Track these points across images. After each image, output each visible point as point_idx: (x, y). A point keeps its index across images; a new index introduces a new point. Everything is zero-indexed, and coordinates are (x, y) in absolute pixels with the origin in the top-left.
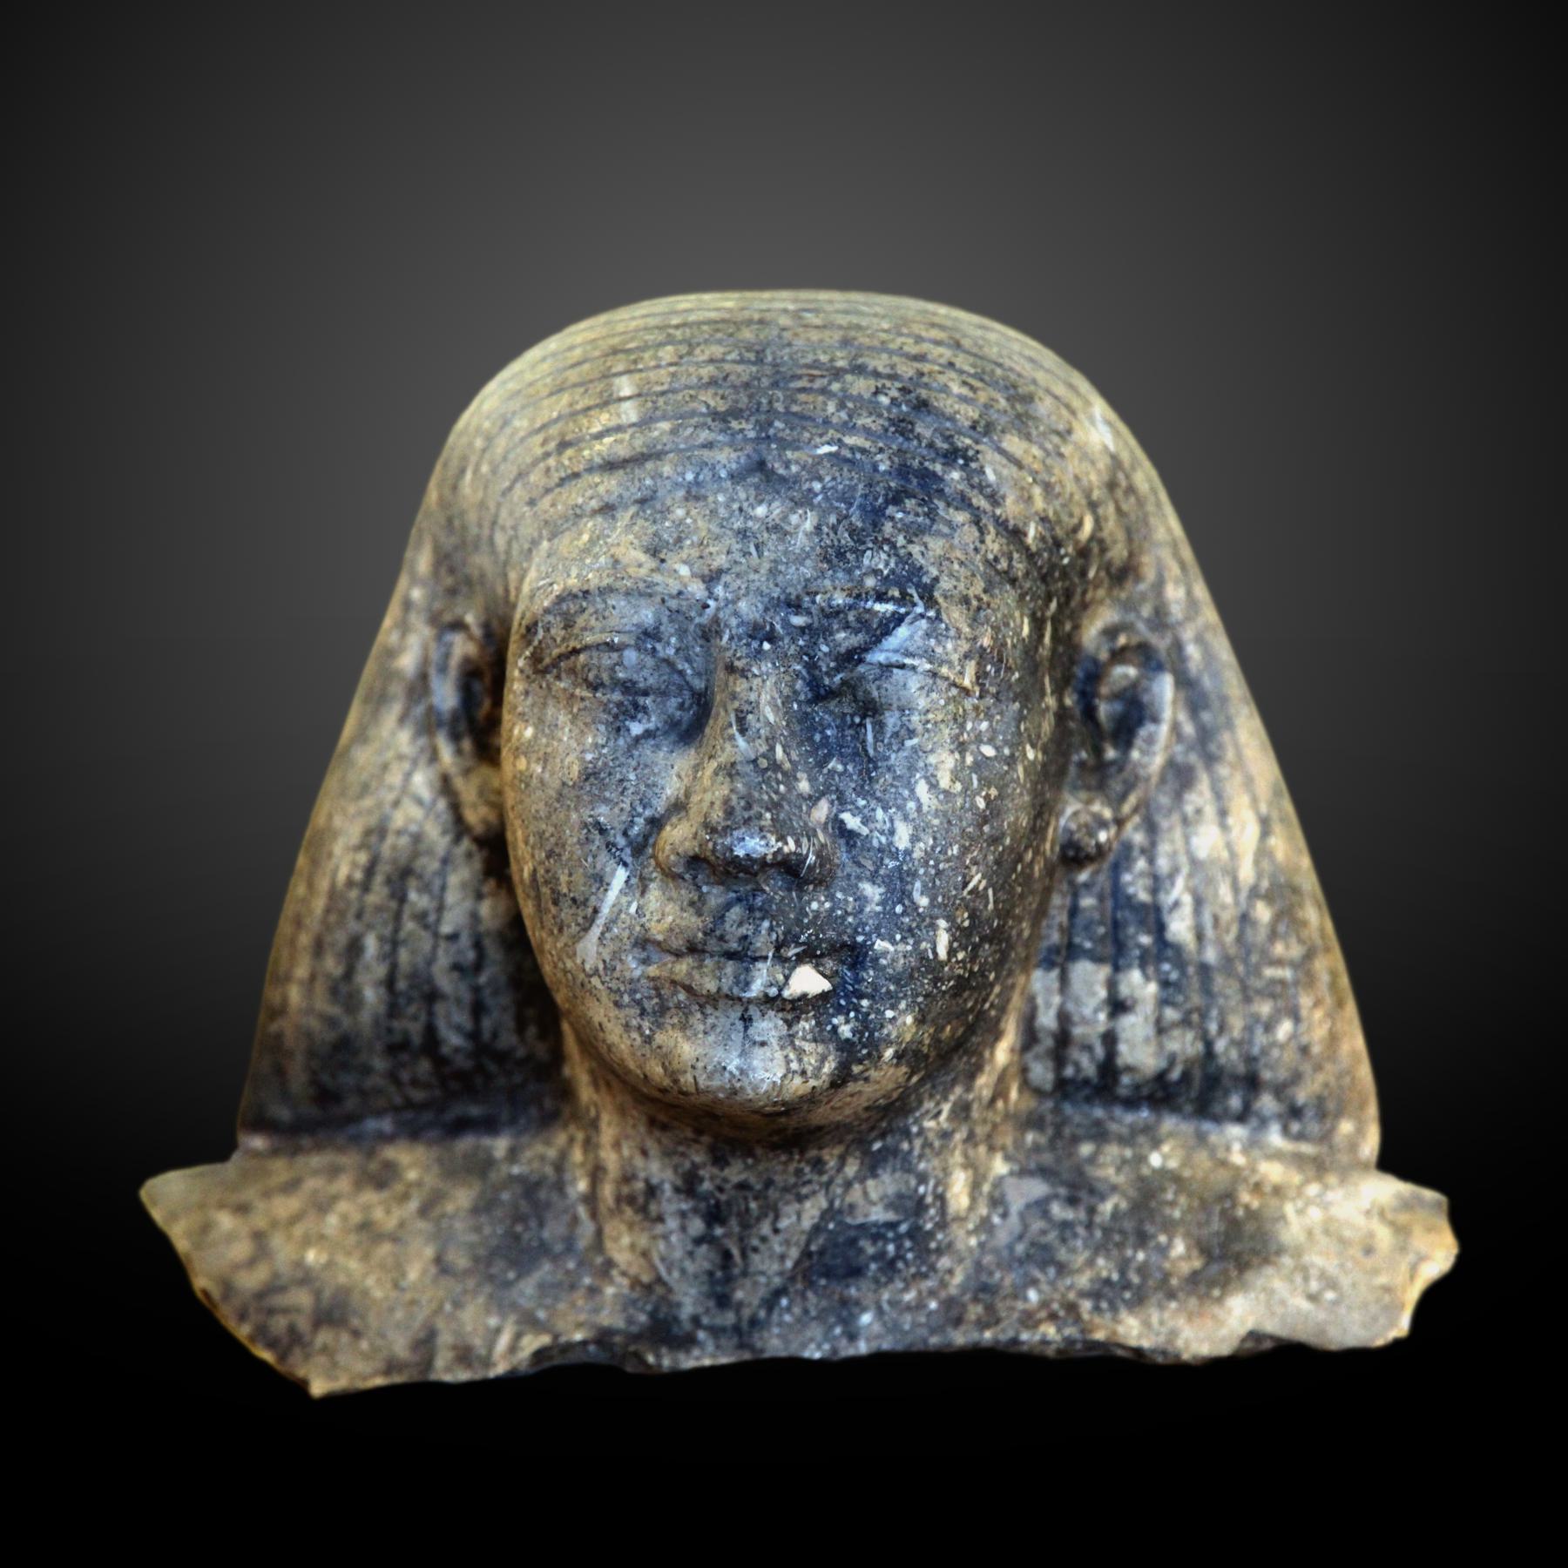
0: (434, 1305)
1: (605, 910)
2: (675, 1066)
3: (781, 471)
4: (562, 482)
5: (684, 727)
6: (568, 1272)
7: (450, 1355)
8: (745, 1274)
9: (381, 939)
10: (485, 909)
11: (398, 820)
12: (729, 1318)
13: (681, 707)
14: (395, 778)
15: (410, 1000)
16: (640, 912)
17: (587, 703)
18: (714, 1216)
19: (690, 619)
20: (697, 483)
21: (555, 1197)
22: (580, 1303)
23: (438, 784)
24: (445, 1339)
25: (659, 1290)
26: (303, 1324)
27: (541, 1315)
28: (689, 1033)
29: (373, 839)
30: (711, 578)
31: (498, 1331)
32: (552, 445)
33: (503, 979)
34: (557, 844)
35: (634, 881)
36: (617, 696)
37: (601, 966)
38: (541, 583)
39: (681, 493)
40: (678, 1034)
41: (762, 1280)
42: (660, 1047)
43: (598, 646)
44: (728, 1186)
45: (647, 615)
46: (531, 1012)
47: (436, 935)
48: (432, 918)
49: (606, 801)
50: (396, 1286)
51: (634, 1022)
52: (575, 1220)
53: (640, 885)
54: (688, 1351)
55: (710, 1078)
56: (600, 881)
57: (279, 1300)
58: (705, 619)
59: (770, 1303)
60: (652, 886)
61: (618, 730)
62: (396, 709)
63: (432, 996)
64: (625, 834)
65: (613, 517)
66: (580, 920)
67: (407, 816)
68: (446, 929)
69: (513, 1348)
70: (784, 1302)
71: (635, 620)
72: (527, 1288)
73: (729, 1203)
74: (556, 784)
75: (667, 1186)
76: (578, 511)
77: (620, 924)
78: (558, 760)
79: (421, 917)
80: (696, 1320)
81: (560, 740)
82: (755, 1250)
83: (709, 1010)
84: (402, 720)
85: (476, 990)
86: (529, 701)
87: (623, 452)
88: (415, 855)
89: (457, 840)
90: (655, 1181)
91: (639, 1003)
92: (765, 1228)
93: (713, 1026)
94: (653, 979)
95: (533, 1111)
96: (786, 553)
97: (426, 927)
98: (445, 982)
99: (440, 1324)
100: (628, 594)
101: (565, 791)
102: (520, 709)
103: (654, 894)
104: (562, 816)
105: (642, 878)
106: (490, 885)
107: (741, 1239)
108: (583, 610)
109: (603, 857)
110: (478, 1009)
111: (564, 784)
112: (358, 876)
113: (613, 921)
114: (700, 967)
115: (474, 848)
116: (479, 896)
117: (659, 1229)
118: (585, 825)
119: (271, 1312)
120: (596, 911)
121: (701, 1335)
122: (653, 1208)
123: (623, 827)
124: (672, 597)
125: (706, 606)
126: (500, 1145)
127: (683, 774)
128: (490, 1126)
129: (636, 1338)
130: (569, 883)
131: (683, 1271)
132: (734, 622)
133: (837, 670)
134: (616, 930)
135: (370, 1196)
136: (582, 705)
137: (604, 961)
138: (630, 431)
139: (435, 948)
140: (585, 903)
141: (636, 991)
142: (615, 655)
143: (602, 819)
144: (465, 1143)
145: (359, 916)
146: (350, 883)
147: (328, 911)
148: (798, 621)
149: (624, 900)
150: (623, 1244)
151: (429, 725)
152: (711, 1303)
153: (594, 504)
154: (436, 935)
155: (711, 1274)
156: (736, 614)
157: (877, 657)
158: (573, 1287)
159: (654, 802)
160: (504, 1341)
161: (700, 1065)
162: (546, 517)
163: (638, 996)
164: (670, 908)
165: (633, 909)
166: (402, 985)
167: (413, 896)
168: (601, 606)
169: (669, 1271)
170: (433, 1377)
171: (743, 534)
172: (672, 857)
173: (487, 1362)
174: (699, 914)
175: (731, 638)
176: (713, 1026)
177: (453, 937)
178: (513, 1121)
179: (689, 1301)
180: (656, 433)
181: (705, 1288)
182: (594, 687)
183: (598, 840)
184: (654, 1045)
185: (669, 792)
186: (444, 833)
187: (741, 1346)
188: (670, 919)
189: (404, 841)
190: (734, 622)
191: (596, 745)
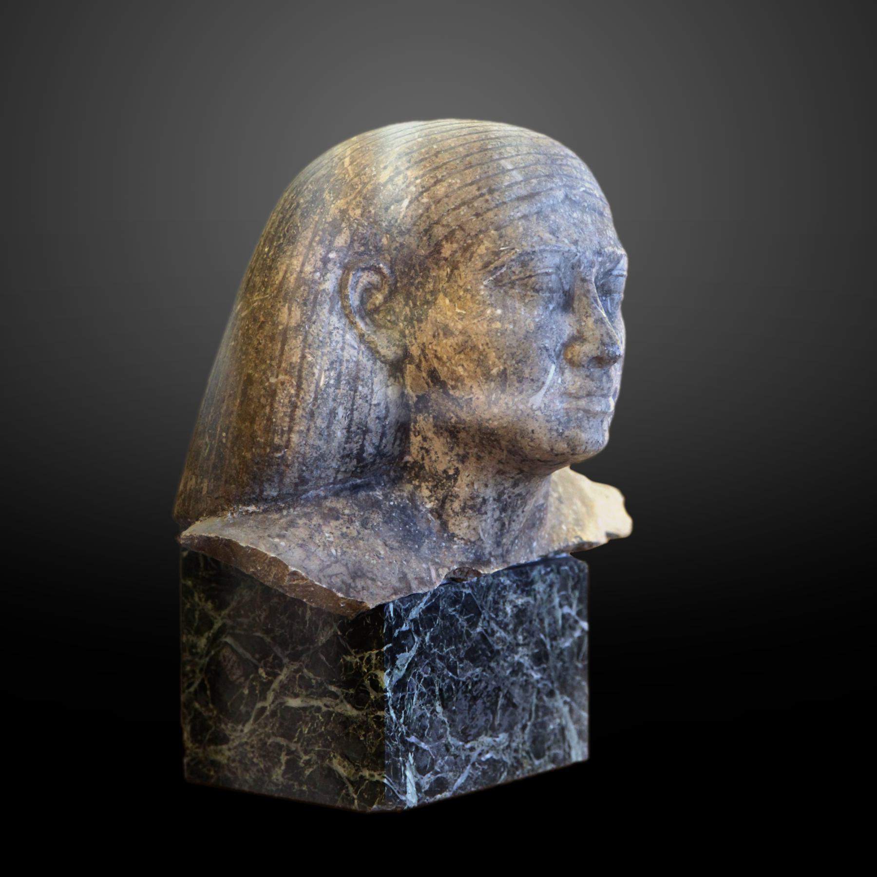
0: (399, 563)
1: (548, 383)
2: (577, 443)
3: (574, 199)
4: (497, 206)
5: (562, 305)
6: (435, 542)
7: (416, 582)
8: (508, 532)
9: (345, 408)
10: (390, 391)
11: (346, 355)
12: (500, 551)
13: (560, 297)
14: (337, 337)
15: (357, 434)
16: (563, 382)
17: (535, 298)
18: (503, 510)
19: (570, 261)
20: (553, 204)
21: (416, 513)
22: (446, 553)
23: (358, 339)
24: (410, 576)
25: (479, 543)
26: (350, 581)
27: (437, 560)
28: (583, 429)
29: (337, 365)
30: (576, 243)
31: (429, 569)
32: (484, 191)
33: (394, 420)
34: (524, 357)
35: (558, 370)
36: (548, 294)
37: (543, 406)
38: (502, 249)
39: (550, 209)
40: (578, 431)
41: (513, 533)
42: (567, 437)
43: (542, 274)
44: (513, 496)
45: (557, 260)
46: (399, 434)
47: (371, 405)
48: (369, 397)
49: (548, 337)
50: (379, 558)
51: (555, 428)
52: (428, 521)
53: (561, 370)
54: (490, 567)
55: (592, 447)
56: (546, 371)
57: (329, 571)
58: (574, 261)
59: (513, 543)
60: (566, 371)
61: (546, 308)
62: (327, 307)
63: (366, 431)
64: (554, 351)
65: (529, 220)
66: (534, 388)
67: (350, 353)
68: (374, 402)
69: (438, 576)
70: (517, 541)
71: (554, 262)
72: (425, 550)
73: (510, 503)
74: (523, 332)
75: (491, 499)
76: (512, 218)
77: (554, 388)
78: (522, 322)
79: (364, 398)
80: (490, 553)
81: (519, 314)
82: (514, 521)
83: (591, 419)
84: (331, 312)
85: (384, 427)
86: (493, 298)
87: (523, 192)
88: (358, 371)
89: (374, 363)
90: (486, 498)
91: (558, 419)
92: (520, 512)
93: (593, 425)
94: (566, 409)
95: (385, 477)
96: (590, 232)
97: (367, 401)
98: (372, 425)
99: (406, 571)
100: (551, 251)
101: (529, 335)
102: (488, 302)
103: (568, 373)
104: (528, 345)
105: (560, 368)
106: (392, 379)
107: (510, 517)
108: (532, 259)
109: (547, 361)
110: (383, 435)
111: (528, 332)
112: (332, 382)
113: (551, 387)
114: (591, 401)
115: (383, 365)
116: (388, 386)
117: (485, 517)
118: (540, 348)
119: (330, 577)
120: (543, 383)
121: (492, 559)
122: (483, 509)
123: (553, 348)
124: (566, 252)
125: (576, 255)
126: (378, 494)
127: (572, 324)
128: (368, 486)
129: (473, 563)
130: (530, 373)
131: (489, 534)
132: (585, 261)
133: (602, 279)
134: (552, 391)
135: (333, 523)
136: (531, 299)
137: (545, 404)
138: (523, 183)
139: (370, 410)
140: (538, 380)
141: (558, 415)
142: (549, 277)
143: (547, 345)
144: (362, 495)
145: (334, 400)
146: (327, 385)
147: (316, 399)
148: (600, 259)
149: (556, 377)
150: (461, 527)
151: (347, 314)
152: (495, 546)
153: (519, 214)
154: (371, 405)
155: (497, 533)
156: (586, 257)
157: (615, 273)
158: (440, 548)
159: (563, 337)
160: (433, 574)
161: (590, 441)
162: (493, 220)
163: (559, 417)
164: (577, 379)
165: (560, 381)
166: (353, 429)
167: (360, 388)
168: (540, 257)
169: (484, 535)
170: (414, 592)
171: (574, 224)
172: (585, 358)
173: (431, 583)
174: (593, 380)
175: (584, 268)
176: (593, 425)
177: (379, 404)
178: (379, 484)
179: (488, 546)
180: (533, 184)
181: (494, 540)
182: (537, 291)
183: (544, 352)
184: (563, 436)
185: (568, 332)
186: (368, 360)
187: (504, 562)
188: (579, 383)
189: (352, 365)
190: (585, 261)
191: (539, 315)
